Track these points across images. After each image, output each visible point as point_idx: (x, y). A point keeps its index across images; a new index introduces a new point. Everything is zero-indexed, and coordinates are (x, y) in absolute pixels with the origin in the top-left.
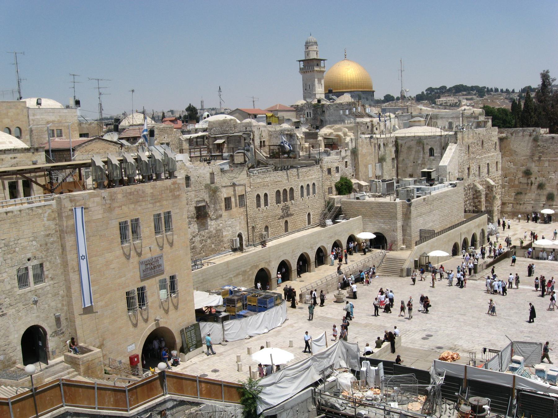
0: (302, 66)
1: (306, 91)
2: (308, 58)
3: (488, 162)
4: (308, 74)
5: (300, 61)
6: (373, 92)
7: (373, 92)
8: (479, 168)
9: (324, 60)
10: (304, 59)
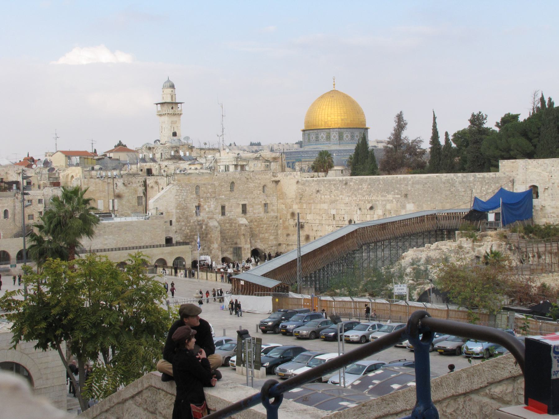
2: (164, 101)
3: (243, 203)
5: (157, 104)
6: (367, 129)
7: (367, 129)
8: (223, 208)
9: (181, 103)
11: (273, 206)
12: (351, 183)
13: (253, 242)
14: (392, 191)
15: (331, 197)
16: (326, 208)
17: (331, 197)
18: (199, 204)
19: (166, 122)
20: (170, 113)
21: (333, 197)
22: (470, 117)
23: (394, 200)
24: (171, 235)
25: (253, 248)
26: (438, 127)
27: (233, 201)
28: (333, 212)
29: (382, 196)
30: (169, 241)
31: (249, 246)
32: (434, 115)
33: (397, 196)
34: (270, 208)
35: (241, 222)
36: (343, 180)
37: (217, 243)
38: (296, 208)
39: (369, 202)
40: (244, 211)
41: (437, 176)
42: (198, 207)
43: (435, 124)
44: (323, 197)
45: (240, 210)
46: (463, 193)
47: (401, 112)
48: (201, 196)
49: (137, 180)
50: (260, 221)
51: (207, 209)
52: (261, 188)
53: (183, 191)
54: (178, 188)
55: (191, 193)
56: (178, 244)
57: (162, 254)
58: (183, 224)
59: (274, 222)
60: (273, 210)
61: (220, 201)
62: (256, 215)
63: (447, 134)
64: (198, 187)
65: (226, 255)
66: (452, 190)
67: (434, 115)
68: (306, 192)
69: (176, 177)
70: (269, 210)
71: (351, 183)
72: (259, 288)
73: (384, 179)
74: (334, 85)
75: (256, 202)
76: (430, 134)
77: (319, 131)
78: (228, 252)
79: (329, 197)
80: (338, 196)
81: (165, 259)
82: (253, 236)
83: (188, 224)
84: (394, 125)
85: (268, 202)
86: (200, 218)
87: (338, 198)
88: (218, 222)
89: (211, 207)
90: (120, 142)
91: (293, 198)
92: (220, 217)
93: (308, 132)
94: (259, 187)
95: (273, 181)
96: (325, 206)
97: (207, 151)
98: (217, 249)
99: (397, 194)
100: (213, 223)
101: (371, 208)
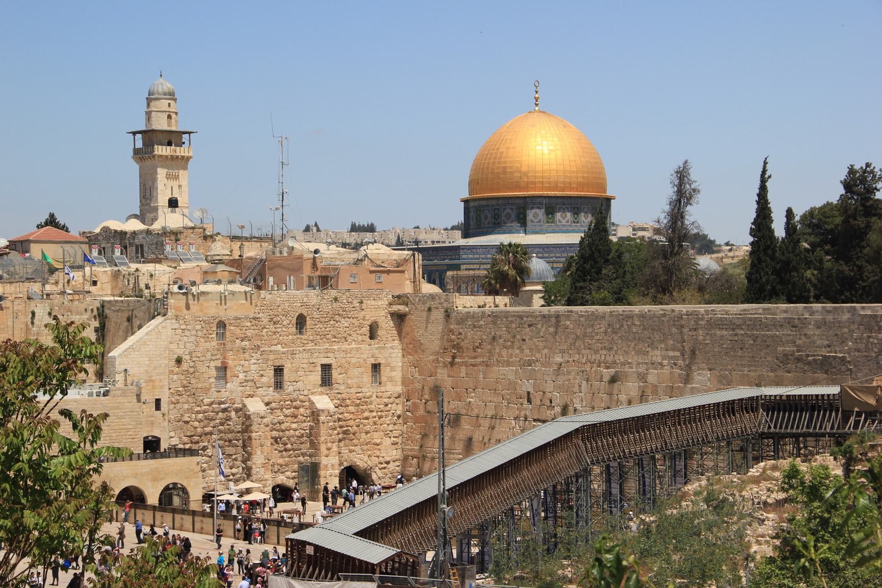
0: (139, 144)
1: (144, 201)
4: (148, 163)
5: (134, 133)
6: (608, 200)
7: (608, 200)
8: (279, 371)
9: (189, 133)
10: (143, 128)
11: (393, 369)
12: (568, 323)
13: (345, 451)
14: (662, 341)
15: (522, 351)
16: (512, 377)
17: (522, 351)
18: (223, 363)
20: (164, 153)
21: (527, 352)
22: (843, 174)
23: (665, 362)
24: (156, 433)
25: (346, 464)
26: (770, 197)
27: (302, 359)
28: (528, 386)
29: (639, 352)
30: (152, 446)
31: (335, 460)
32: (764, 172)
33: (671, 353)
34: (385, 372)
35: (319, 406)
36: (550, 316)
37: (262, 452)
38: (443, 376)
39: (608, 368)
40: (326, 380)
41: (764, 309)
42: (223, 369)
43: (763, 189)
44: (504, 352)
45: (316, 377)
46: (824, 352)
47: (686, 162)
48: (229, 346)
49: (83, 307)
50: (362, 402)
51: (242, 376)
52: (366, 330)
53: (187, 333)
54: (177, 326)
55: (206, 337)
56: (175, 452)
57: (135, 476)
58: (186, 406)
59: (394, 406)
60: (391, 380)
61: (272, 357)
62: (353, 390)
63: (790, 213)
64: (222, 325)
65: (281, 479)
66: (799, 342)
67: (764, 172)
68: (466, 341)
70: (384, 379)
71: (568, 323)
72: (347, 564)
73: (642, 316)
74: (537, 99)
75: (354, 360)
76: (751, 213)
77: (500, 202)
78: (288, 473)
79: (517, 351)
80: (539, 352)
81: (141, 487)
82: (346, 435)
83: (199, 409)
84: (670, 192)
85: (382, 361)
86: (224, 395)
87: (538, 356)
88: (267, 404)
89: (250, 367)
90: (52, 216)
91: (438, 353)
92: (271, 393)
93: (476, 204)
94: (361, 326)
95: (392, 314)
96: (509, 372)
97: (246, 244)
98: (264, 465)
99: (673, 349)
100: (255, 406)
101: (613, 380)
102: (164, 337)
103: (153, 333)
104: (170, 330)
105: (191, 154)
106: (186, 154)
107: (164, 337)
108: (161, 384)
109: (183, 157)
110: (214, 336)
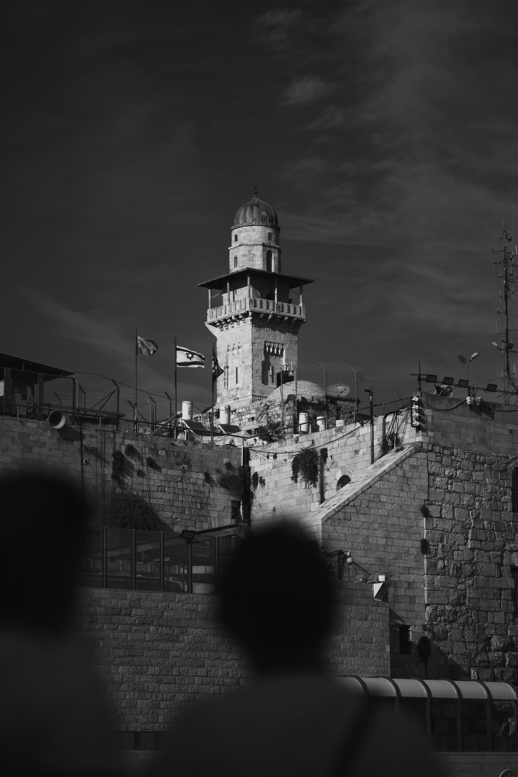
19: (247, 347)
20: (264, 310)
69: (428, 412)
102: (414, 489)
103: (393, 478)
104: (425, 475)
105: (303, 316)
106: (297, 315)
107: (414, 489)
108: (410, 593)
109: (291, 318)
110: (508, 497)
